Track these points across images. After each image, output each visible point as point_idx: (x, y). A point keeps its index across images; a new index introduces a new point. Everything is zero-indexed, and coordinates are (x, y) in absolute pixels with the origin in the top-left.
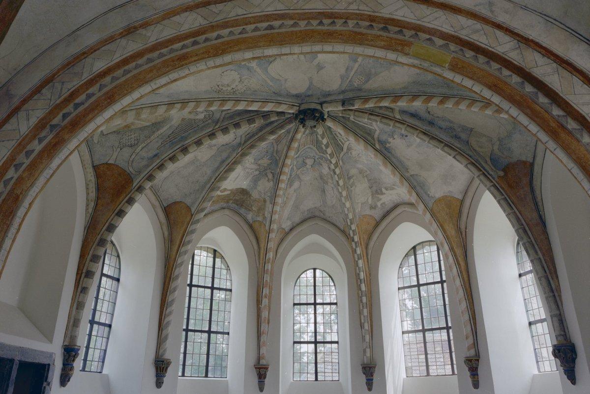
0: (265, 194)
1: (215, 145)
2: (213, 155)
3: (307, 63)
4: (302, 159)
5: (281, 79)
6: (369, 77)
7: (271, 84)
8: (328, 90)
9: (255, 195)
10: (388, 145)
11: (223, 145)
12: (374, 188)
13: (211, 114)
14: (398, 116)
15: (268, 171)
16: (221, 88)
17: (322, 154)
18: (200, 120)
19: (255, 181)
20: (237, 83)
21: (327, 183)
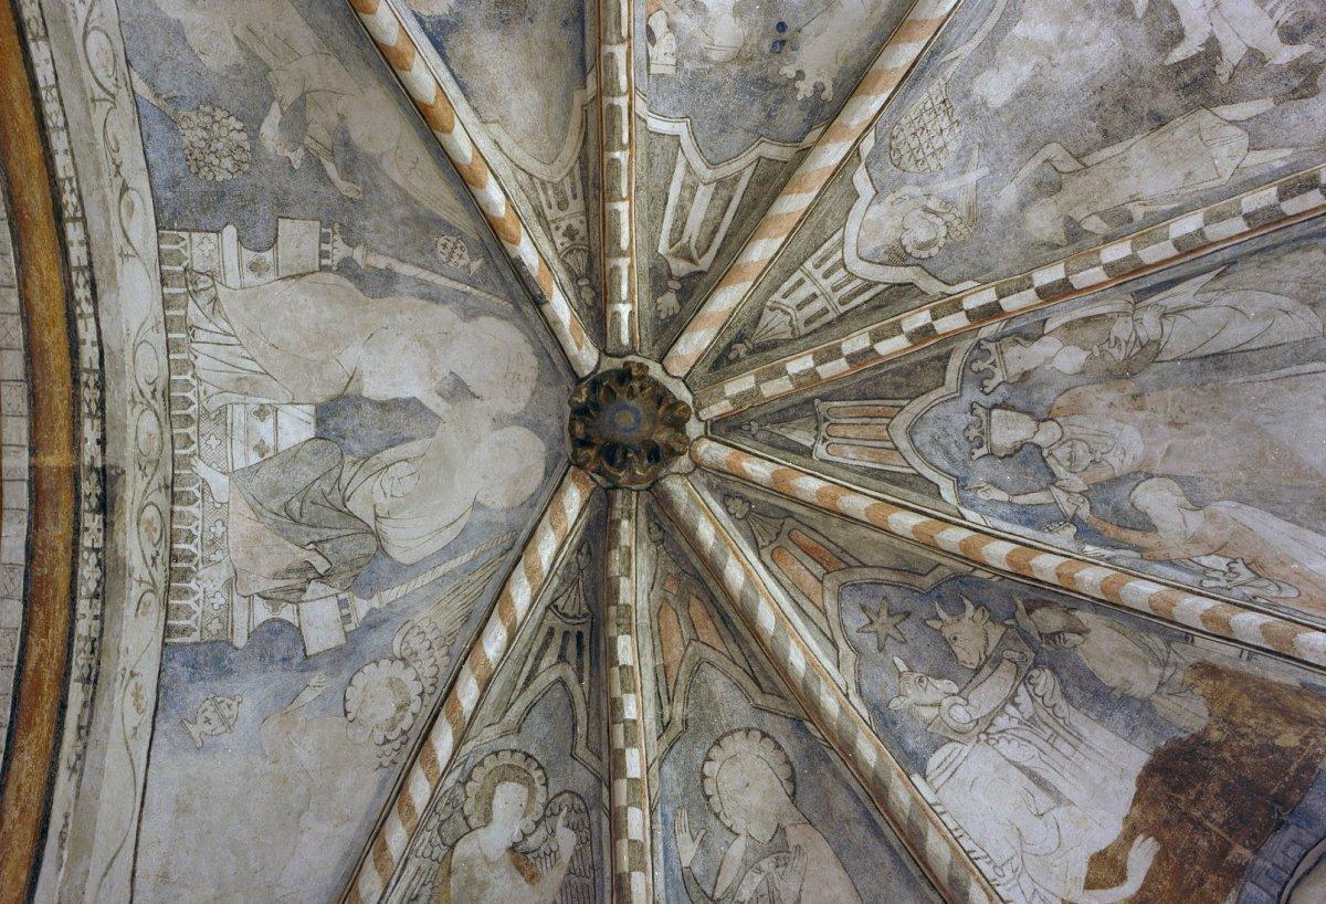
0: (1165, 664)
1: (780, 829)
2: (838, 855)
3: (438, 433)
4: (982, 461)
5: (462, 523)
6: (427, 225)
7: (465, 558)
8: (534, 361)
9: (1191, 715)
10: (828, 94)
11: (793, 796)
12: (1167, 101)
13: (569, 802)
14: (591, 85)
15: (1026, 623)
16: (397, 732)
17: (952, 375)
18: (578, 853)
19: (1098, 697)
20: (407, 676)
21: (1150, 352)
